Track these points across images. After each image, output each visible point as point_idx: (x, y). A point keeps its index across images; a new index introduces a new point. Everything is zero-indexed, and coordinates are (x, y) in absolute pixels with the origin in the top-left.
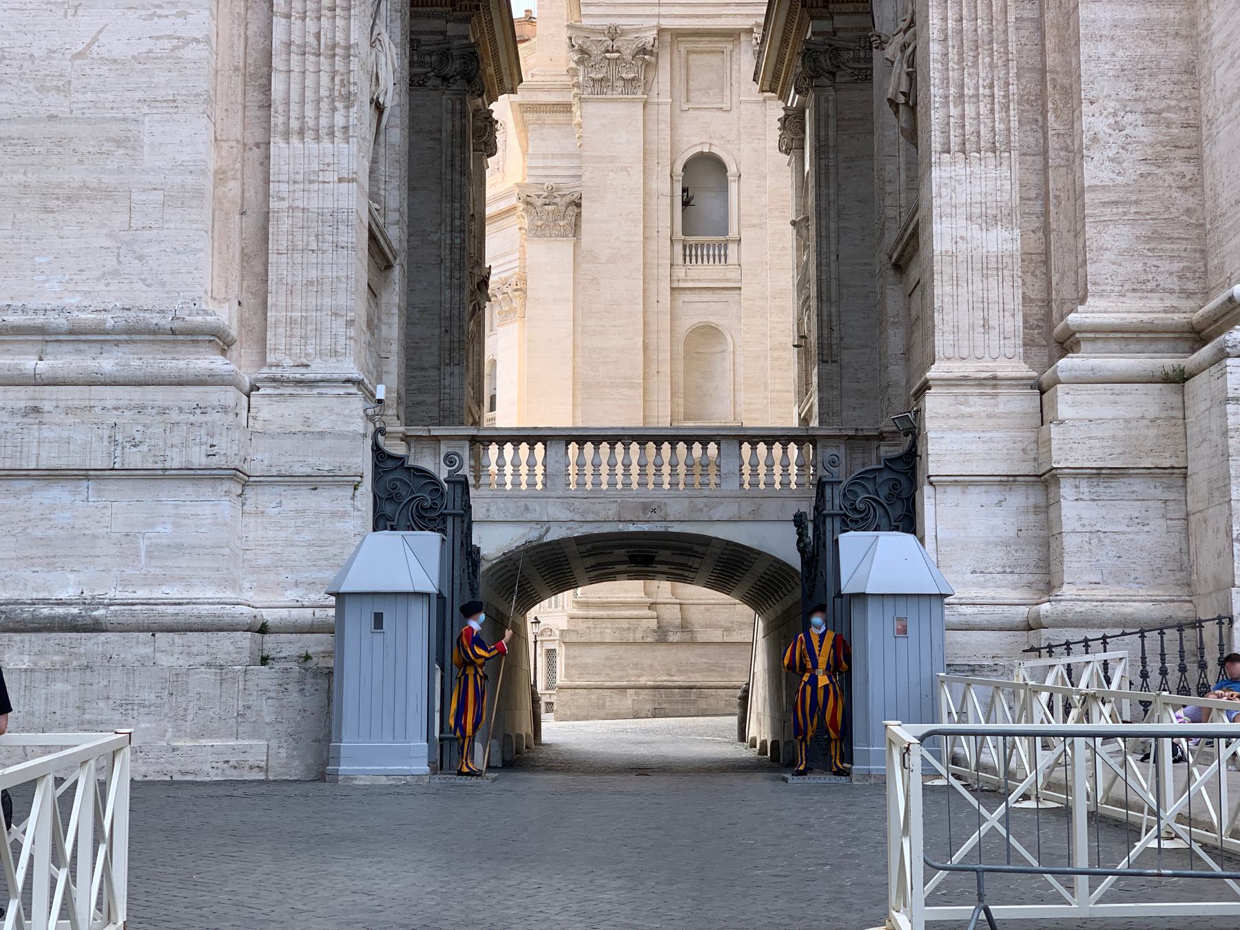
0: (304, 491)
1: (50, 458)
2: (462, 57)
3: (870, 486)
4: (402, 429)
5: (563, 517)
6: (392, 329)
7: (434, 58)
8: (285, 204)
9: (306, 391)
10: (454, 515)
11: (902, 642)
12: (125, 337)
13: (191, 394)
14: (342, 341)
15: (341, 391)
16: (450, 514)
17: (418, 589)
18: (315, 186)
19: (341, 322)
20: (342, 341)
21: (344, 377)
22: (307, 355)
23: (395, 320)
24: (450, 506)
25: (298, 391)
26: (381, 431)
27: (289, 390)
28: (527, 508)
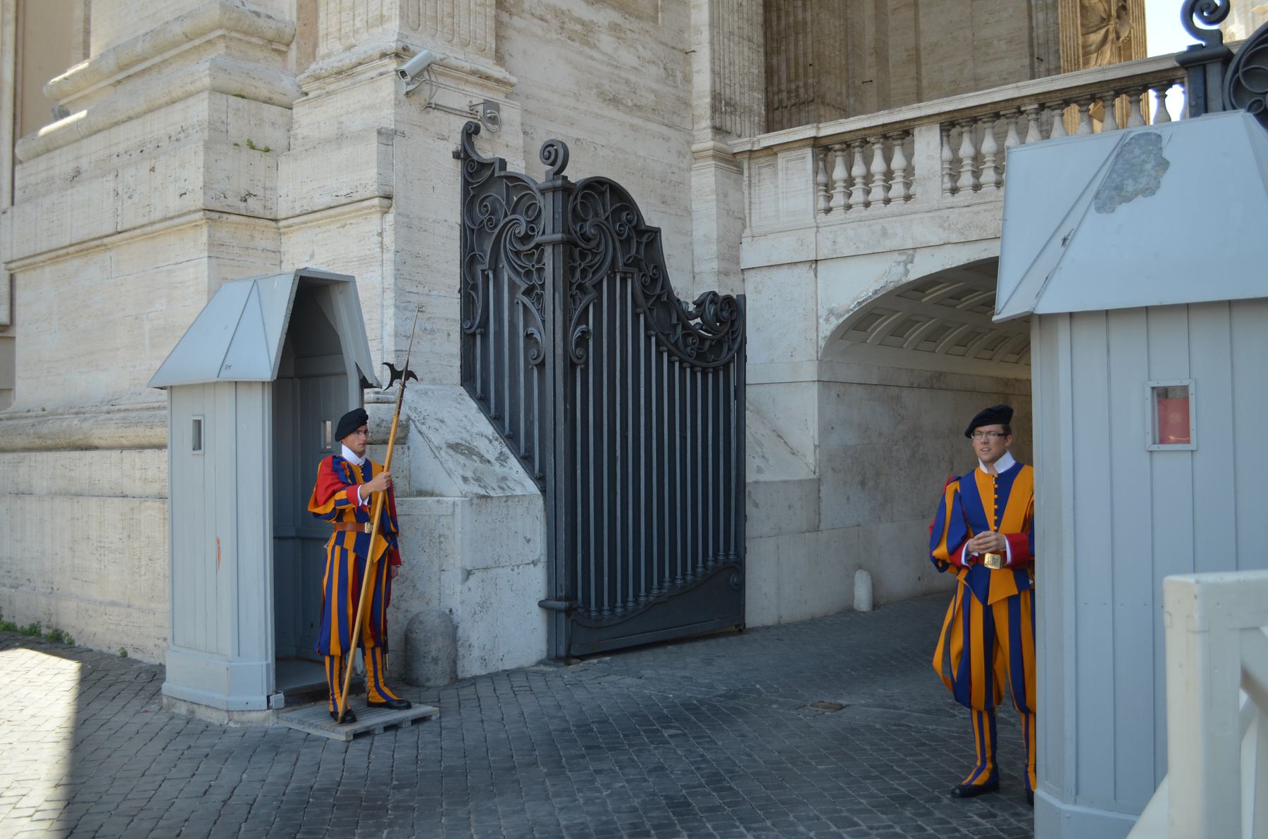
4: (710, 144)
5: (934, 240)
9: (348, 82)
10: (554, 244)
12: (158, 59)
15: (374, 73)
16: (548, 243)
21: (377, 53)
22: (356, 32)
25: (343, 84)
27: (332, 87)
28: (884, 233)
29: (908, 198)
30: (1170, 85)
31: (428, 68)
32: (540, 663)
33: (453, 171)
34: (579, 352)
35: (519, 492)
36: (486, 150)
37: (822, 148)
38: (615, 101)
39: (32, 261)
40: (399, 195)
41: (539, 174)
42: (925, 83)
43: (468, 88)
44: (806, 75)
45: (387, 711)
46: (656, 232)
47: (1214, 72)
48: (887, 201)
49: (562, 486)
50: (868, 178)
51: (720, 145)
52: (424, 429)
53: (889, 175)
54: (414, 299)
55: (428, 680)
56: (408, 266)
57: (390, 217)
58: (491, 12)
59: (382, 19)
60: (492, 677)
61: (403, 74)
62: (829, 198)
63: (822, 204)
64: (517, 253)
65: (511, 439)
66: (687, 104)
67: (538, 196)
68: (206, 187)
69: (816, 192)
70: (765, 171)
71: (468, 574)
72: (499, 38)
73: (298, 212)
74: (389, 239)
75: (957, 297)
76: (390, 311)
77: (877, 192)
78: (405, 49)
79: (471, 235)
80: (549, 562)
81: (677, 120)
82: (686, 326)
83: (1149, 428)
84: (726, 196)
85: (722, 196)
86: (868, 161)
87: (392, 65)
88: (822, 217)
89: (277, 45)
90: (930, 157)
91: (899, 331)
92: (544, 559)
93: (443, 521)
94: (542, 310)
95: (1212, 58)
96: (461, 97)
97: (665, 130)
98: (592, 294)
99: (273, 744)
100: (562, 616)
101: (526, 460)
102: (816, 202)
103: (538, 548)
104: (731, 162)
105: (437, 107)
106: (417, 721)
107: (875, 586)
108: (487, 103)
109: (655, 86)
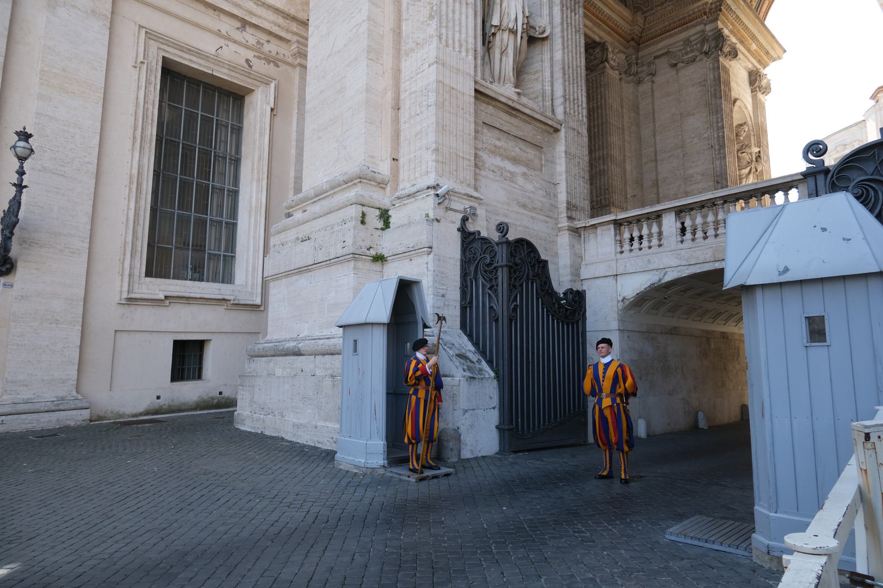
0: (407, 261)
1: (298, 263)
2: (714, 39)
3: (870, 167)
6: (561, 166)
7: (698, 45)
8: (408, 93)
9: (413, 199)
10: (502, 267)
11: (818, 352)
12: (332, 192)
13: (341, 214)
14: (430, 164)
17: (368, 321)
18: (420, 75)
19: (430, 152)
20: (430, 164)
23: (563, 160)
24: (500, 261)
26: (465, 220)
28: (649, 262)
29: (660, 246)
30: (790, 188)
31: (448, 193)
33: (457, 236)
34: (513, 314)
35: (487, 376)
36: (471, 227)
37: (618, 224)
38: (524, 206)
39: (277, 277)
40: (435, 246)
41: (495, 236)
42: (661, 196)
43: (464, 201)
44: (605, 194)
46: (546, 262)
47: (821, 178)
48: (650, 247)
49: (506, 373)
50: (641, 238)
51: (571, 224)
52: (445, 347)
53: (650, 235)
54: (442, 292)
56: (439, 276)
57: (431, 256)
58: (473, 168)
59: (427, 173)
60: (476, 458)
61: (437, 195)
62: (622, 247)
63: (619, 249)
64: (486, 271)
65: (483, 353)
66: (556, 207)
67: (496, 247)
68: (354, 244)
69: (616, 244)
70: (592, 236)
71: (466, 411)
72: (475, 180)
74: (431, 267)
75: (685, 291)
77: (645, 243)
78: (438, 185)
79: (465, 263)
80: (500, 408)
81: (551, 214)
82: (559, 304)
83: (805, 336)
84: (574, 247)
85: (572, 247)
86: (640, 230)
87: (432, 192)
88: (619, 255)
89: (381, 184)
90: (670, 227)
91: (656, 307)
92: (498, 406)
93: (455, 388)
94: (497, 296)
95: (819, 172)
96: (460, 205)
97: (546, 218)
98: (520, 289)
99: (386, 482)
100: (507, 432)
101: (490, 362)
102: (616, 249)
103: (495, 402)
104: (576, 232)
105: (451, 209)
106: (447, 475)
107: (648, 426)
108: (471, 207)
109: (542, 199)
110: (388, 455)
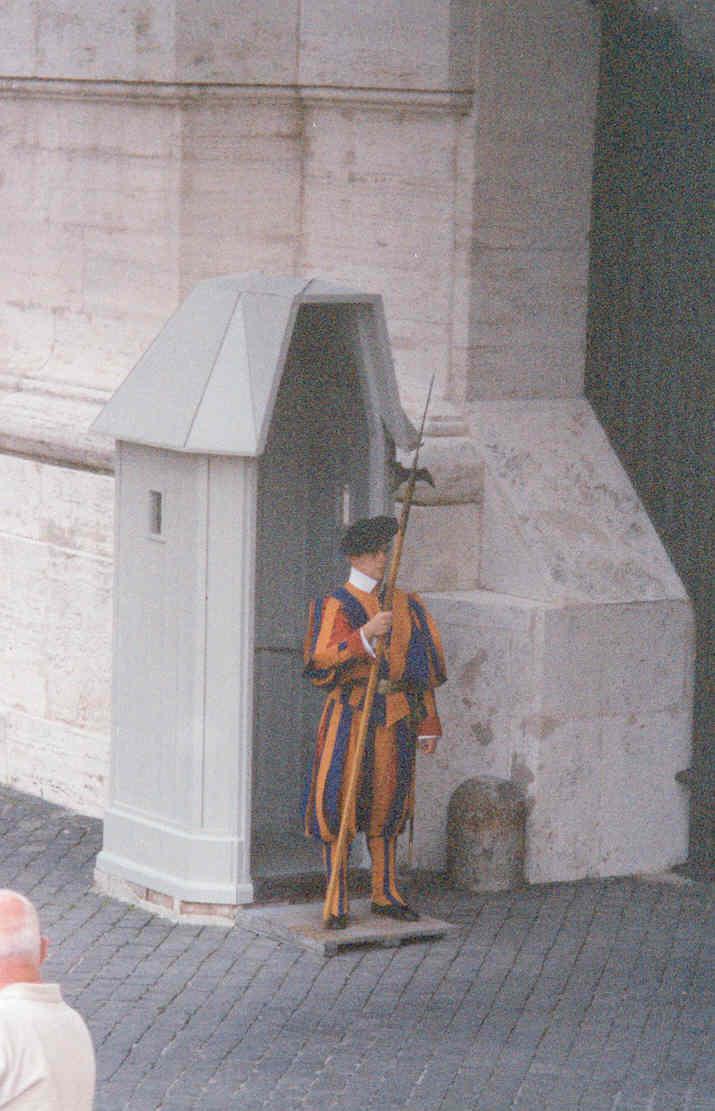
32: (676, 869)
45: (389, 921)
55: (477, 881)
65: (654, 500)
73: (329, 82)
76: (464, 283)
92: (689, 703)
110: (254, 864)
